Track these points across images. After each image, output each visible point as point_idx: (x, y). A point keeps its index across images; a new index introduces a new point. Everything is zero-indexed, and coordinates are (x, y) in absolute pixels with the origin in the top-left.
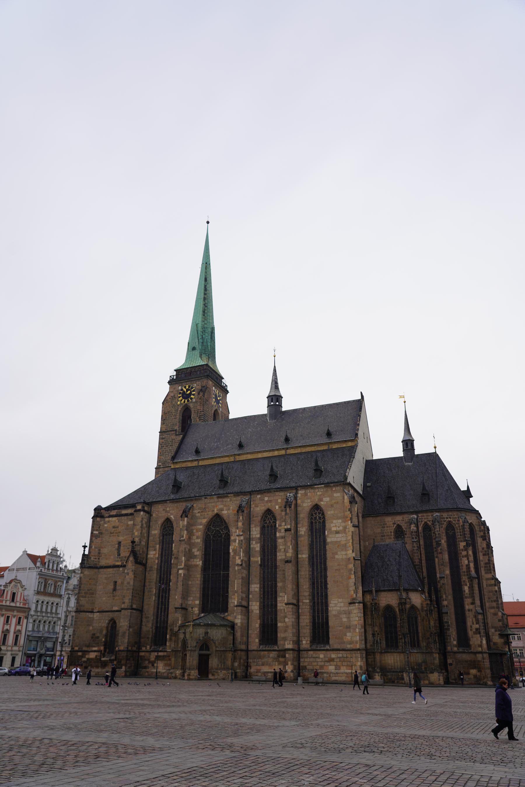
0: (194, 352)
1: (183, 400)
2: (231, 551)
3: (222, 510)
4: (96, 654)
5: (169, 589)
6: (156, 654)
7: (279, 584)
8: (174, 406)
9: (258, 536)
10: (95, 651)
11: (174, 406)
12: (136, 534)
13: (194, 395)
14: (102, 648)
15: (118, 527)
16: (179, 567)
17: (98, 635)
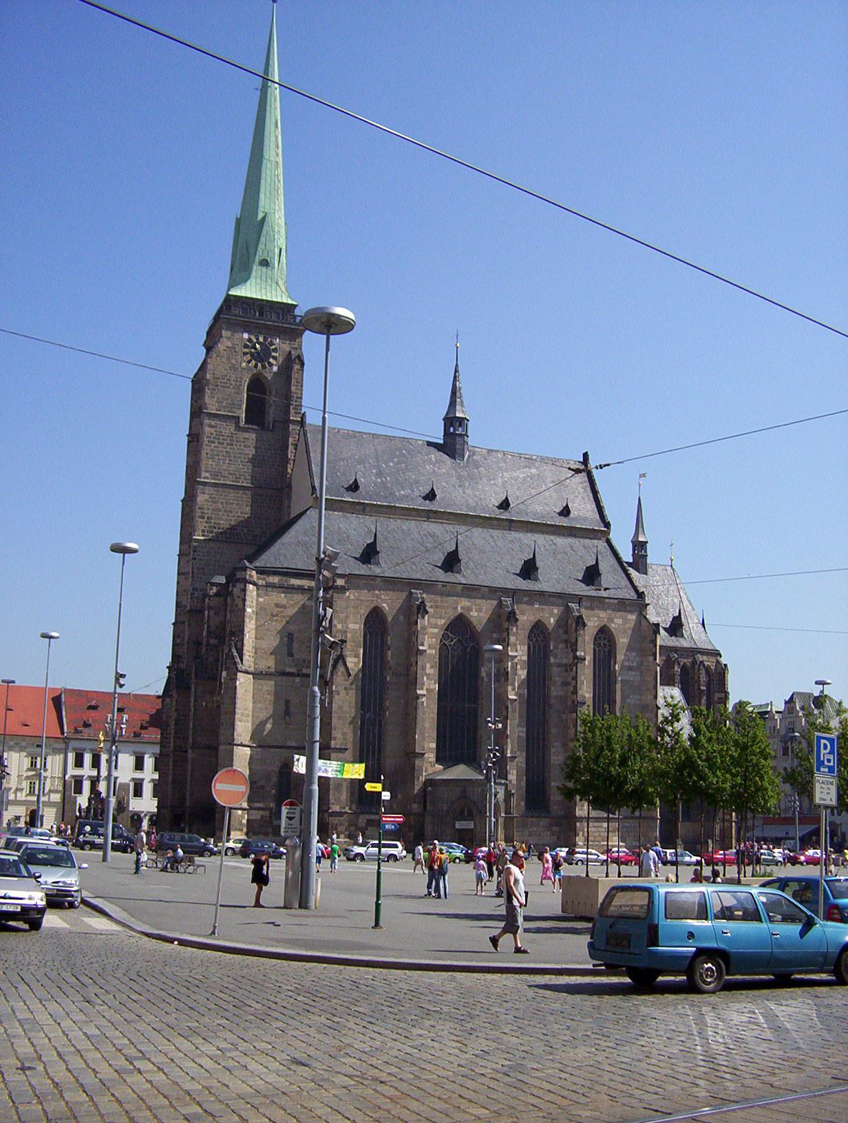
0: (264, 269)
1: (254, 362)
2: (483, 674)
3: (470, 609)
4: (261, 813)
5: (380, 721)
6: (367, 817)
7: (553, 731)
8: (233, 368)
9: (525, 658)
10: (259, 809)
11: (233, 368)
12: (339, 626)
13: (275, 358)
14: (272, 805)
15: (284, 607)
16: (419, 692)
17: (262, 783)
